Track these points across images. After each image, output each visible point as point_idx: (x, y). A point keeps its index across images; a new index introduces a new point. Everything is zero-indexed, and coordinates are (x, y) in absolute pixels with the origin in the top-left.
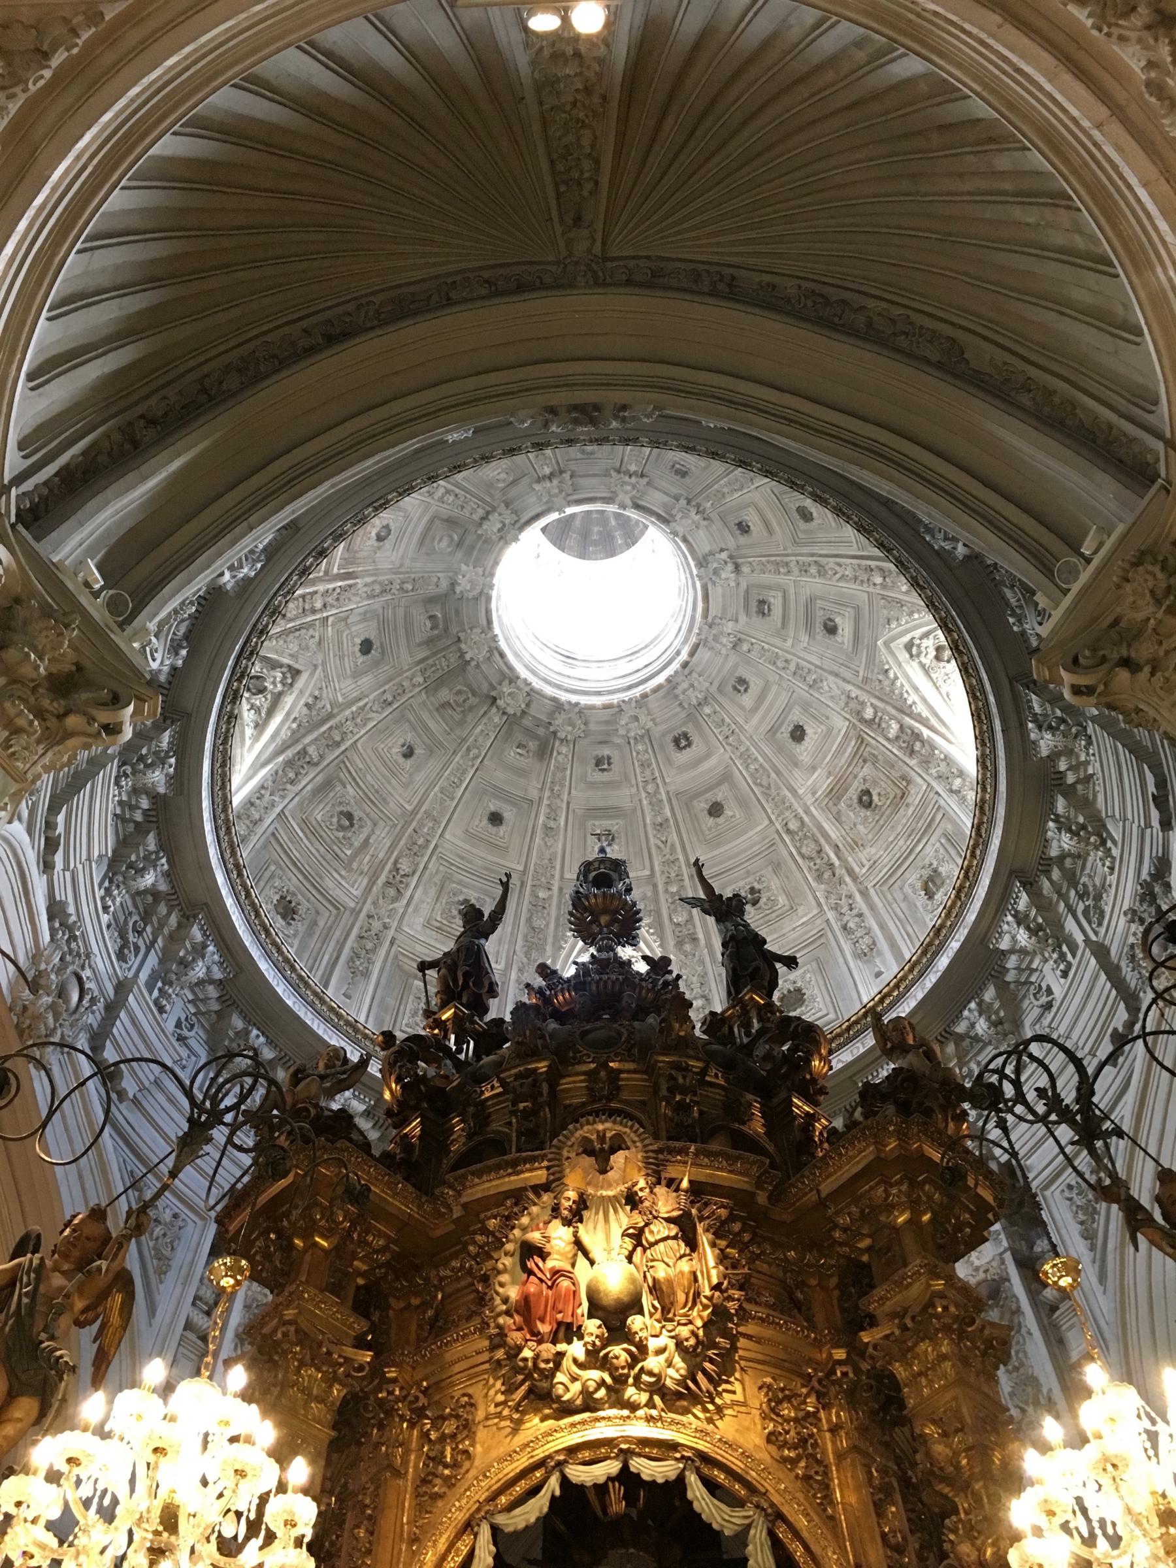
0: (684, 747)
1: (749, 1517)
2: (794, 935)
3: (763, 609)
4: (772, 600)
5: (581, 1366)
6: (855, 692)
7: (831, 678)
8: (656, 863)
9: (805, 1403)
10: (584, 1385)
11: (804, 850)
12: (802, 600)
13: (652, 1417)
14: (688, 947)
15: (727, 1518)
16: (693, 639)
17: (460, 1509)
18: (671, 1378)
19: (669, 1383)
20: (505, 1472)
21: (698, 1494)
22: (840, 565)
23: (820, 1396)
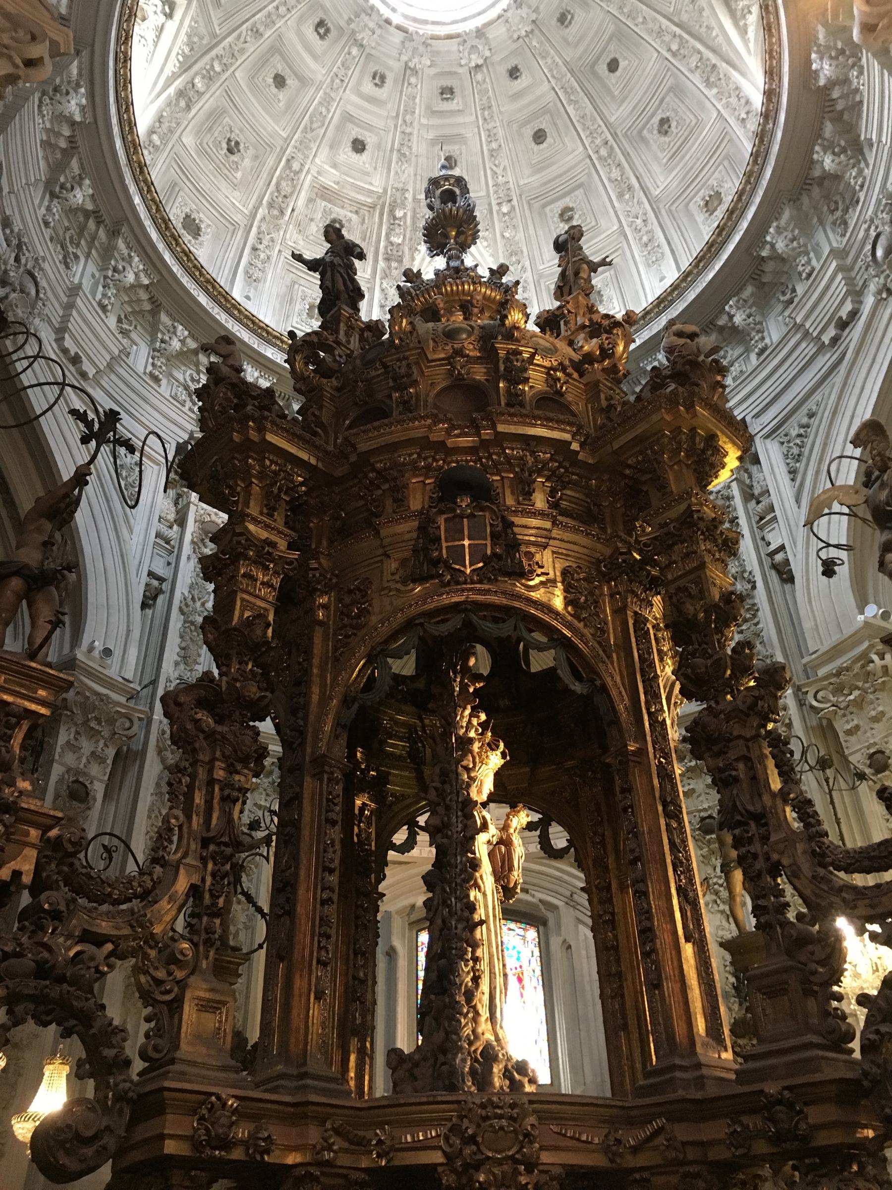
0: (319, 34)
2: (221, 197)
3: (447, 92)
4: (455, 101)
6: (409, 196)
7: (411, 170)
8: (230, 39)
11: (284, 184)
12: (462, 131)
14: (183, 104)
16: (411, 27)
22: (505, 169)
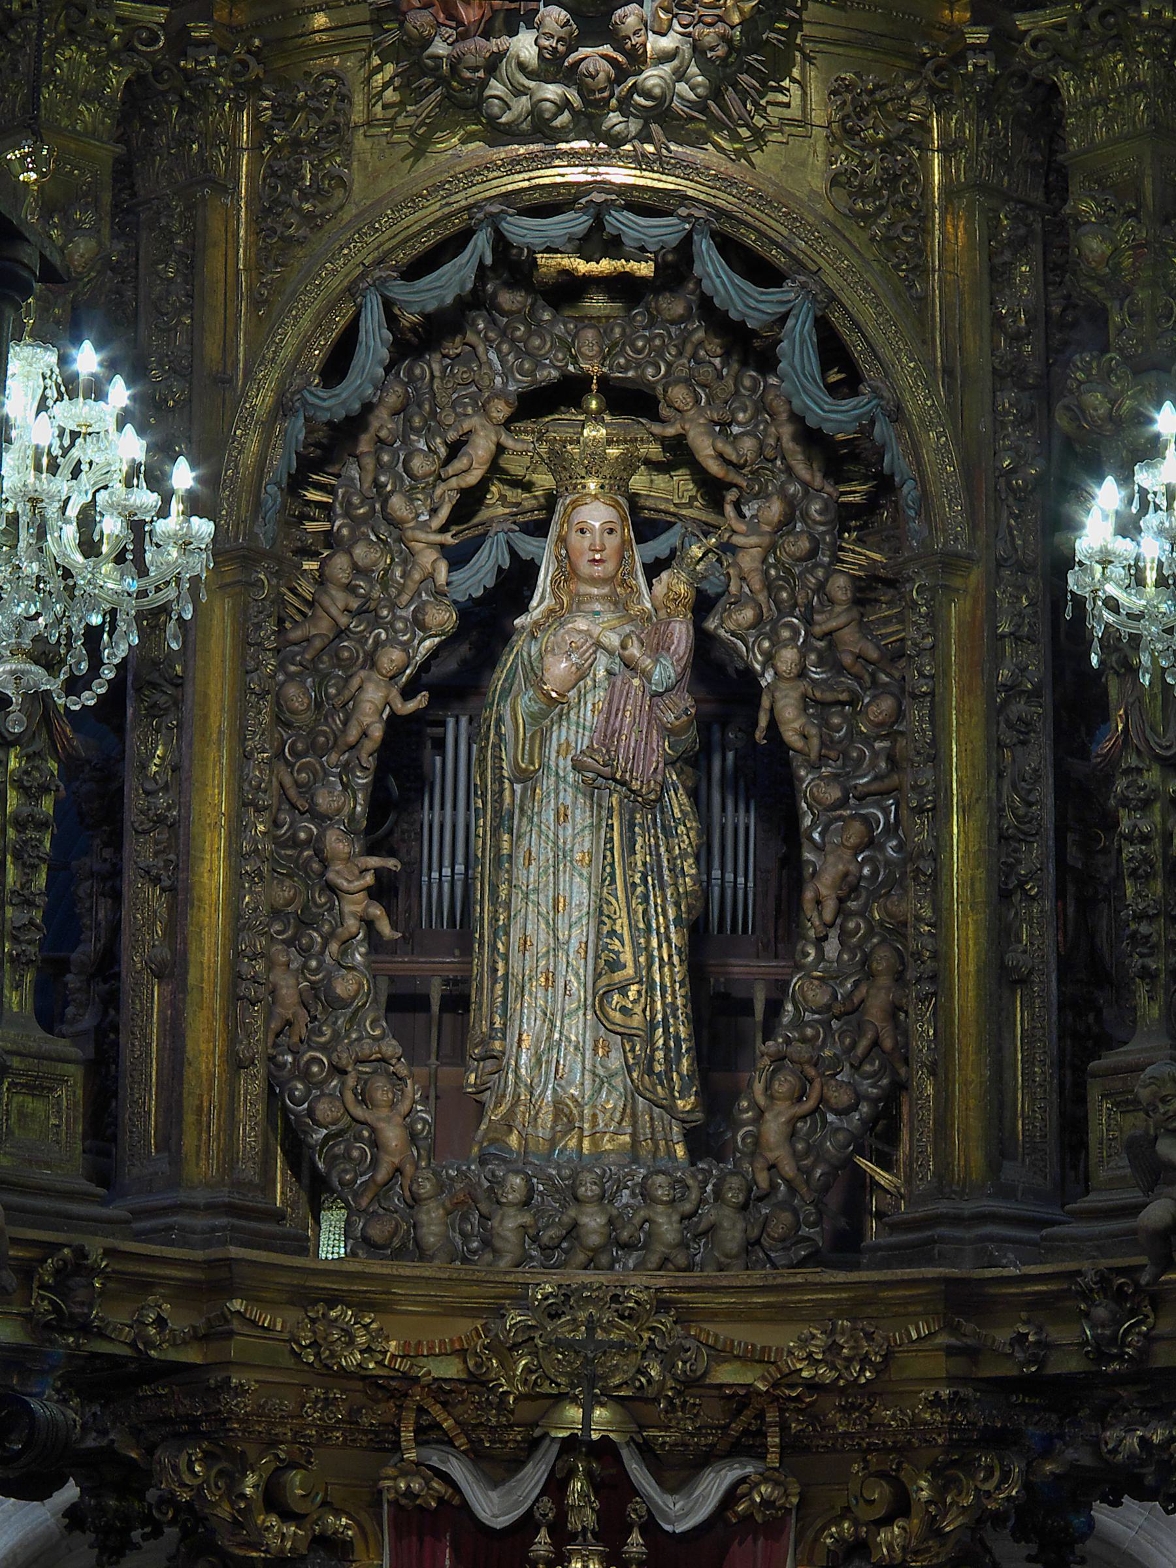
1: (789, 301)
5: (531, 75)
9: (907, 107)
10: (536, 106)
13: (644, 155)
15: (752, 303)
17: (334, 273)
18: (681, 98)
19: (676, 103)
20: (404, 223)
21: (710, 269)
23: (933, 91)
